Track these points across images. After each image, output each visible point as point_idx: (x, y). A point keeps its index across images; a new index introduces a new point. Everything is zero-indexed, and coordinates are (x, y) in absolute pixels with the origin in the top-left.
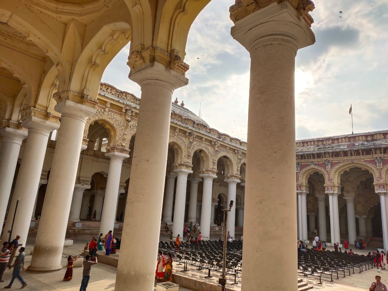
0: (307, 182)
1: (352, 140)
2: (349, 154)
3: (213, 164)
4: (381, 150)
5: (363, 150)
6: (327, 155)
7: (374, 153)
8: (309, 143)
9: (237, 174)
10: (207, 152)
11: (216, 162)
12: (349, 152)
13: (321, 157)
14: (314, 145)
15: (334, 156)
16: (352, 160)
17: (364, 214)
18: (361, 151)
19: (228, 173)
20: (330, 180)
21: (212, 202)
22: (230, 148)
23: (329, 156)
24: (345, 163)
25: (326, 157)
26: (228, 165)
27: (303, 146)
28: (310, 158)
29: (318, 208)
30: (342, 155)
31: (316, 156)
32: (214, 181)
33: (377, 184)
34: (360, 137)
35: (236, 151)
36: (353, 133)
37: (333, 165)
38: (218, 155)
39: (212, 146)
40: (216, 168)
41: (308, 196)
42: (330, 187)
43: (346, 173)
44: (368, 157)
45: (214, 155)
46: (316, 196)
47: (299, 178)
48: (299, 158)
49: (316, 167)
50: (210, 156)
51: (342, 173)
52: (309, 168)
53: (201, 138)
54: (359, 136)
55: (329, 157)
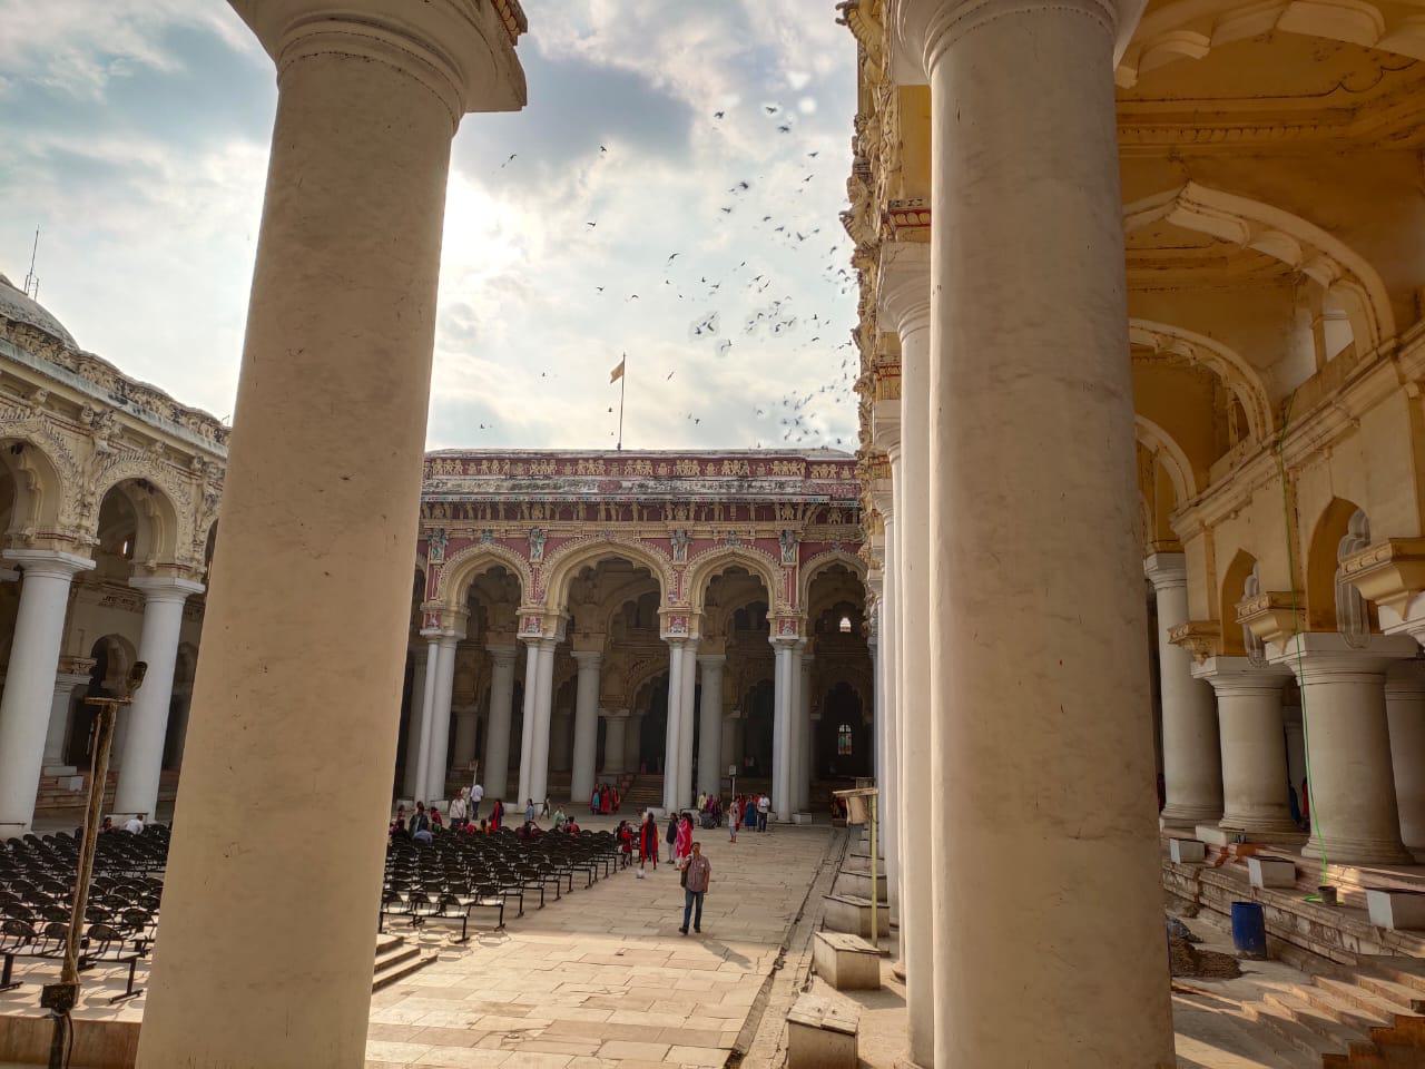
0: (463, 600)
2: (603, 514)
3: (78, 510)
4: (688, 510)
5: (642, 506)
6: (536, 513)
7: (670, 517)
8: (485, 465)
9: (192, 559)
10: (55, 456)
11: (96, 502)
12: (602, 507)
14: (500, 473)
16: (607, 533)
17: (624, 706)
18: (635, 508)
19: (152, 551)
20: (539, 596)
21: (59, 671)
22: (167, 447)
23: (541, 516)
24: (585, 542)
26: (151, 519)
27: (465, 472)
28: (483, 518)
29: (489, 690)
30: (581, 514)
31: (502, 513)
32: (79, 581)
33: (667, 613)
34: (639, 461)
35: (196, 465)
36: (619, 446)
37: (551, 544)
38: (110, 473)
39: (79, 428)
40: (95, 529)
41: (462, 647)
42: (533, 618)
43: (587, 574)
44: (654, 529)
45: (88, 468)
46: (489, 647)
47: (440, 587)
48: (444, 515)
49: (499, 550)
50: (67, 472)
51: (575, 573)
52: (475, 550)
53: (27, 390)
54: (635, 459)
55: (543, 518)
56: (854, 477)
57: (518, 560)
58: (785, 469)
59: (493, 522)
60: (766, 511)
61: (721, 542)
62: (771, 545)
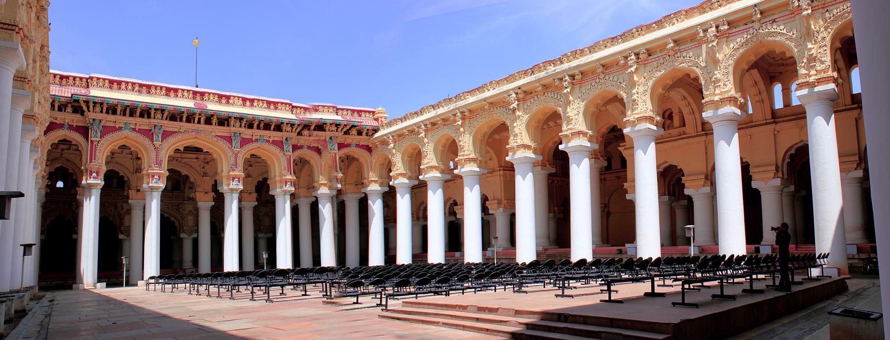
1: (198, 97)
28: (124, 115)
30: (184, 119)
37: (166, 135)
44: (223, 131)
47: (97, 154)
49: (134, 135)
52: (119, 134)
57: (146, 141)
59: (131, 119)
60: (279, 127)
61: (256, 140)
62: (279, 144)
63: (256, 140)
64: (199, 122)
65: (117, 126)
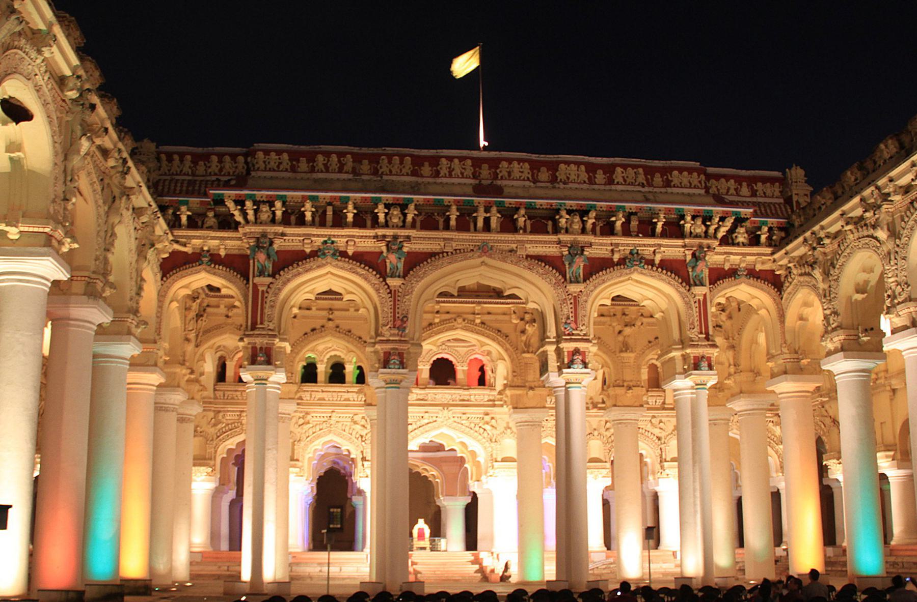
2: (480, 223)
13: (369, 223)
14: (340, 171)
15: (418, 224)
23: (401, 224)
25: (390, 224)
27: (293, 169)
28: (323, 224)
30: (453, 223)
34: (515, 164)
37: (415, 262)
47: (267, 311)
56: (754, 194)
58: (685, 181)
63: (622, 262)
64: (487, 228)
65: (308, 251)
